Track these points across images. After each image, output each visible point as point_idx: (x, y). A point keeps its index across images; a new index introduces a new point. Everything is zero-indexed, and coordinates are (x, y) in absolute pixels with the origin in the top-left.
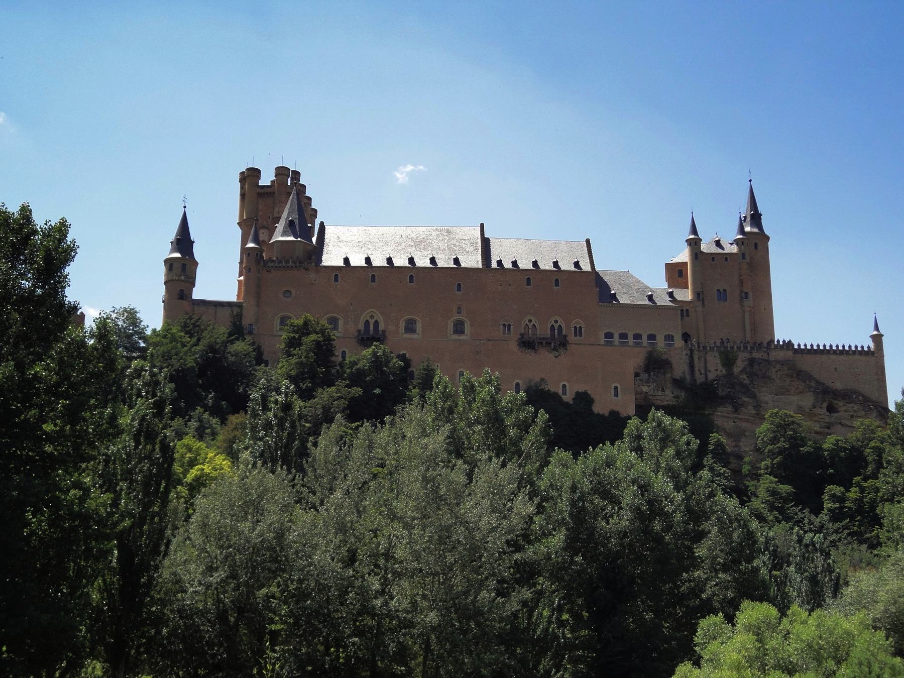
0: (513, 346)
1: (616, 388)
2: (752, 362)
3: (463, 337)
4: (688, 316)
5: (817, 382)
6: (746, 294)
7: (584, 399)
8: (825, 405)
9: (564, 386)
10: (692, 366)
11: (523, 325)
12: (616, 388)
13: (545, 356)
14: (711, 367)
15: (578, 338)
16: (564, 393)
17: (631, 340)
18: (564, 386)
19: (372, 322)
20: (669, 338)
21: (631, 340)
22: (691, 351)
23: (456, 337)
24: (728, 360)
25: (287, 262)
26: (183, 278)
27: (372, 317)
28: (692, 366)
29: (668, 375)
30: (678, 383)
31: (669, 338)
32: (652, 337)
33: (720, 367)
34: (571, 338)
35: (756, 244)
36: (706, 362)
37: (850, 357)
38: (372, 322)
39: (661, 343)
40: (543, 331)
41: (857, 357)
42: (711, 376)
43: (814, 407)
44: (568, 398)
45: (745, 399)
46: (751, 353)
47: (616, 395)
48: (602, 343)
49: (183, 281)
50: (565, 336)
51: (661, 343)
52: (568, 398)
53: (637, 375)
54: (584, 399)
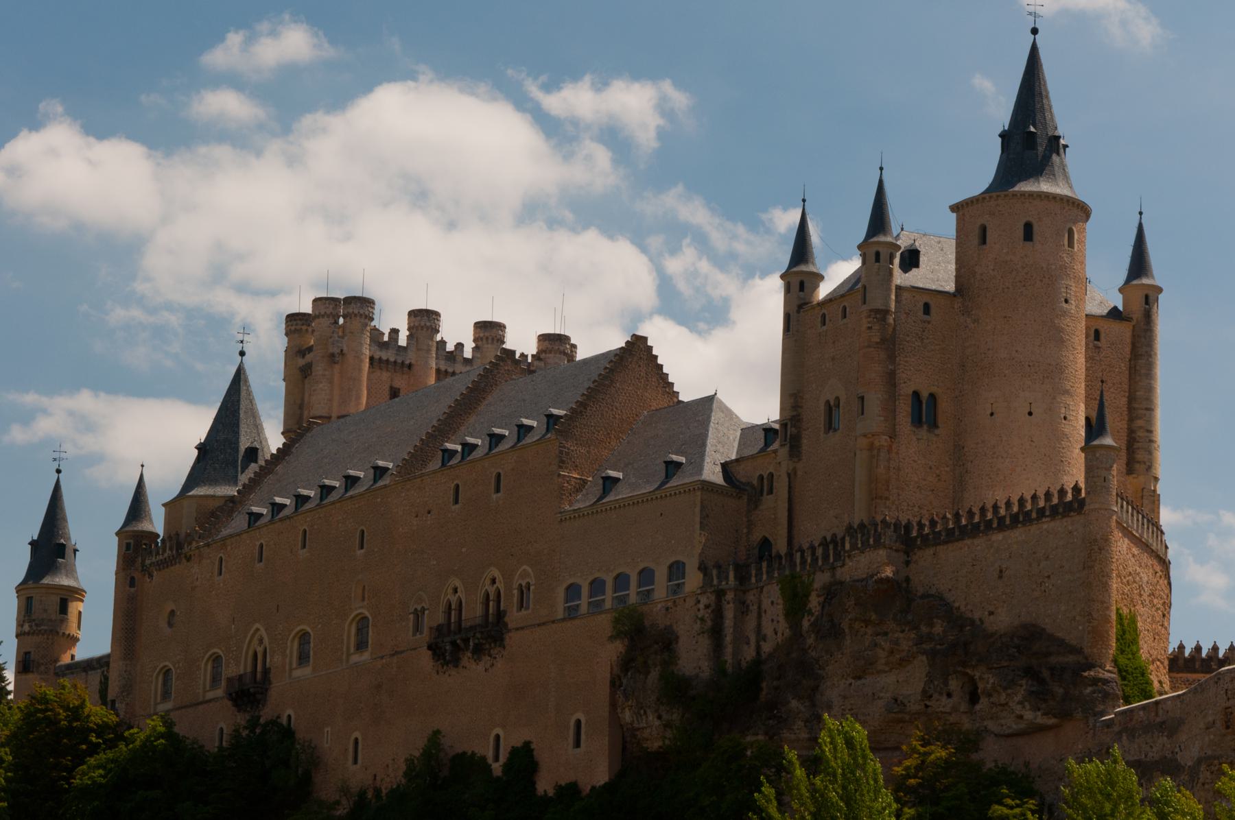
0: (425, 657)
1: (578, 722)
2: (831, 593)
3: (366, 656)
4: (770, 492)
5: (956, 619)
6: (862, 398)
7: (524, 761)
8: (954, 684)
9: (498, 737)
10: (716, 633)
11: (442, 608)
12: (578, 722)
13: (473, 669)
14: (768, 629)
15: (524, 612)
16: (496, 759)
17: (609, 597)
18: (498, 737)
19: (260, 650)
20: (677, 570)
21: (609, 597)
22: (720, 594)
23: (355, 658)
24: (795, 603)
25: (164, 551)
26: (26, 628)
27: (261, 641)
28: (716, 633)
29: (654, 674)
30: (677, 690)
31: (677, 570)
32: (646, 576)
33: (783, 626)
34: (514, 617)
35: (984, 229)
36: (759, 616)
37: (1034, 529)
38: (260, 650)
39: (660, 589)
40: (473, 612)
41: (1047, 525)
42: (767, 648)
43: (926, 695)
44: (497, 768)
45: (794, 704)
46: (833, 568)
47: (577, 744)
48: (560, 614)
49: (28, 634)
50: (505, 612)
51: (660, 589)
52: (497, 768)
53: (615, 684)
54: (524, 761)
